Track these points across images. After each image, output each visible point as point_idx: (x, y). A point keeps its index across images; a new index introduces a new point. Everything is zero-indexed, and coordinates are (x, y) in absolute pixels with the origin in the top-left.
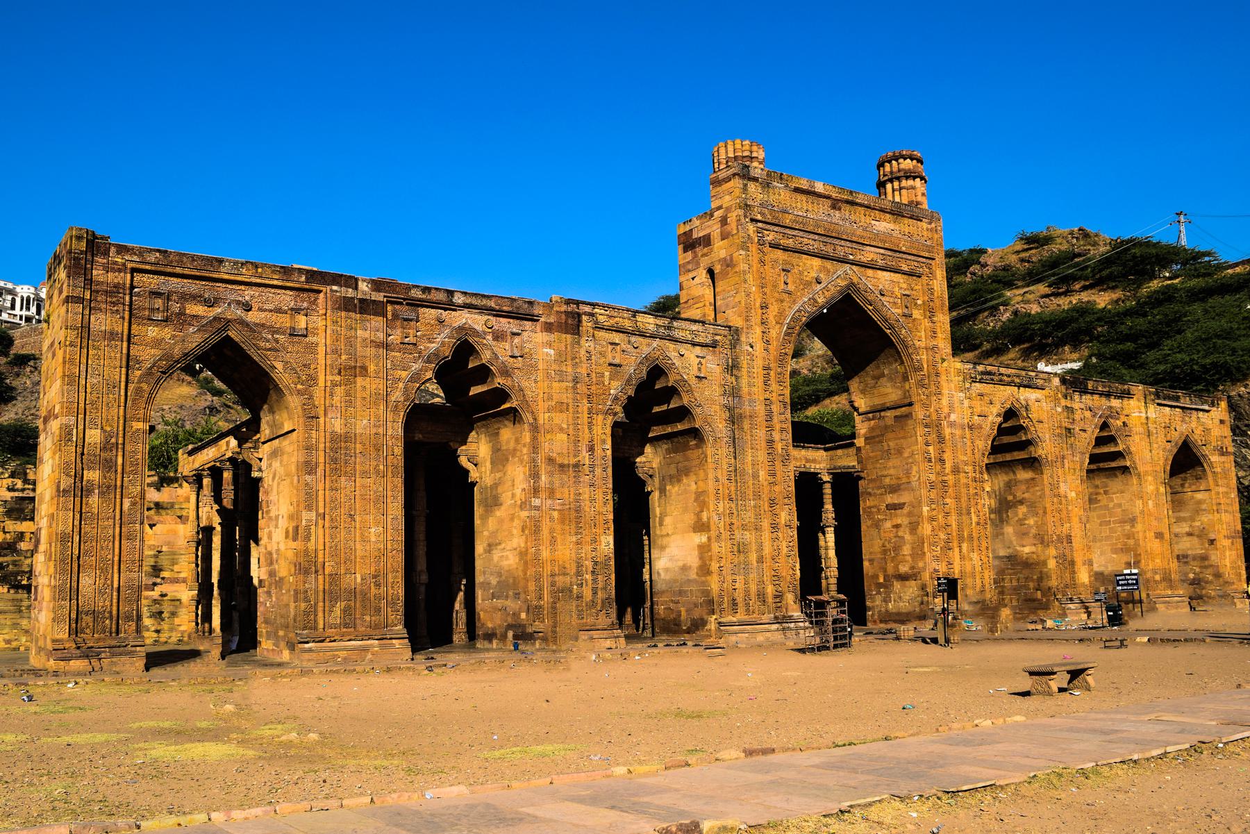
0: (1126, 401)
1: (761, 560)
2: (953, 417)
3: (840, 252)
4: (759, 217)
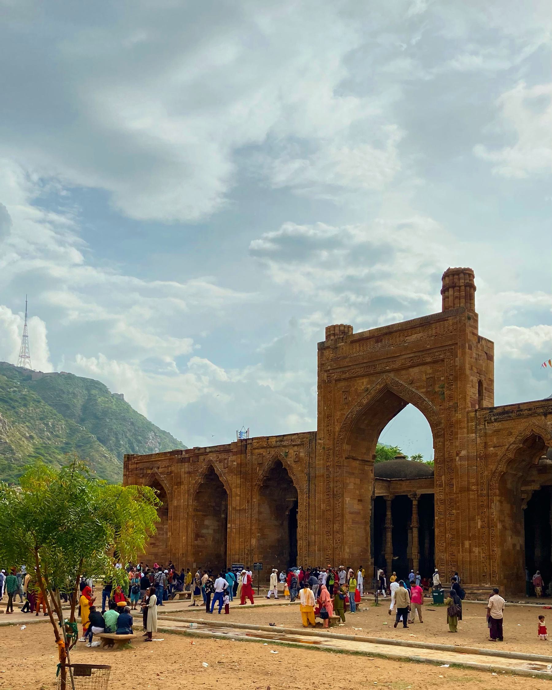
2: (463, 453)
3: (379, 369)
4: (329, 368)
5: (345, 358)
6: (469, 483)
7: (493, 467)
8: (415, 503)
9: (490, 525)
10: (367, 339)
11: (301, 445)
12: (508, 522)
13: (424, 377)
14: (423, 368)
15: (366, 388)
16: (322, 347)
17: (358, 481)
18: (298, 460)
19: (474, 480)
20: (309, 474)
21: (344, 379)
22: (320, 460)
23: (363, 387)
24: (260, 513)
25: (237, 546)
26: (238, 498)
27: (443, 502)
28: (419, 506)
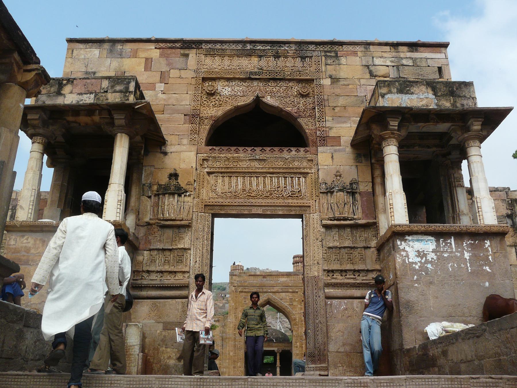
3: (265, 290)
10: (258, 275)
13: (288, 298)
20: (222, 337)
21: (245, 292)
22: (229, 330)
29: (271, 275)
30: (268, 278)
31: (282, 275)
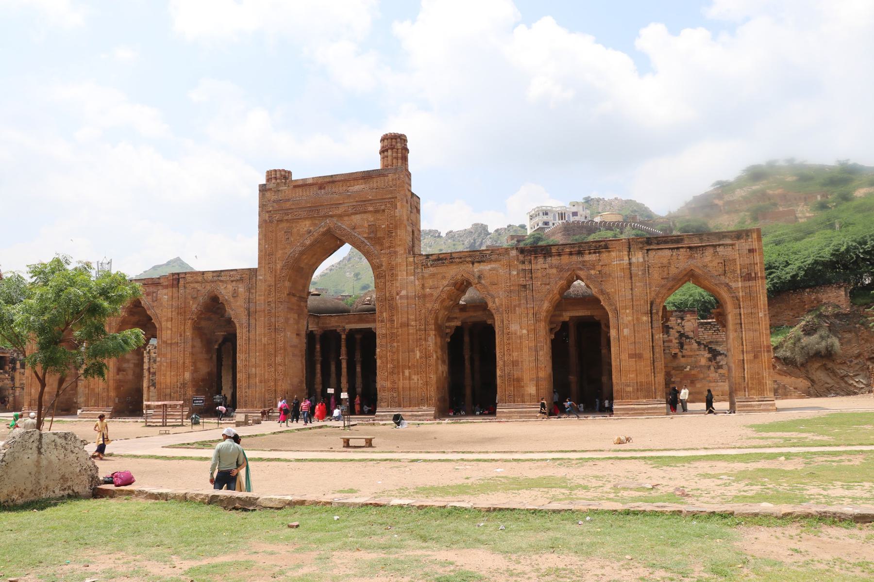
0: (604, 255)
1: (261, 382)
2: (404, 293)
3: (322, 213)
5: (289, 200)
6: (408, 319)
7: (429, 306)
8: (343, 336)
9: (427, 356)
11: (241, 280)
12: (440, 353)
13: (366, 225)
14: (365, 216)
15: (306, 230)
16: (263, 189)
17: (296, 316)
18: (235, 294)
19: (412, 317)
20: (248, 309)
23: (306, 229)
24: (193, 347)
25: (168, 381)
26: (169, 332)
27: (385, 336)
28: (347, 340)
29: (333, 182)
30: (329, 189)
31: (355, 179)
